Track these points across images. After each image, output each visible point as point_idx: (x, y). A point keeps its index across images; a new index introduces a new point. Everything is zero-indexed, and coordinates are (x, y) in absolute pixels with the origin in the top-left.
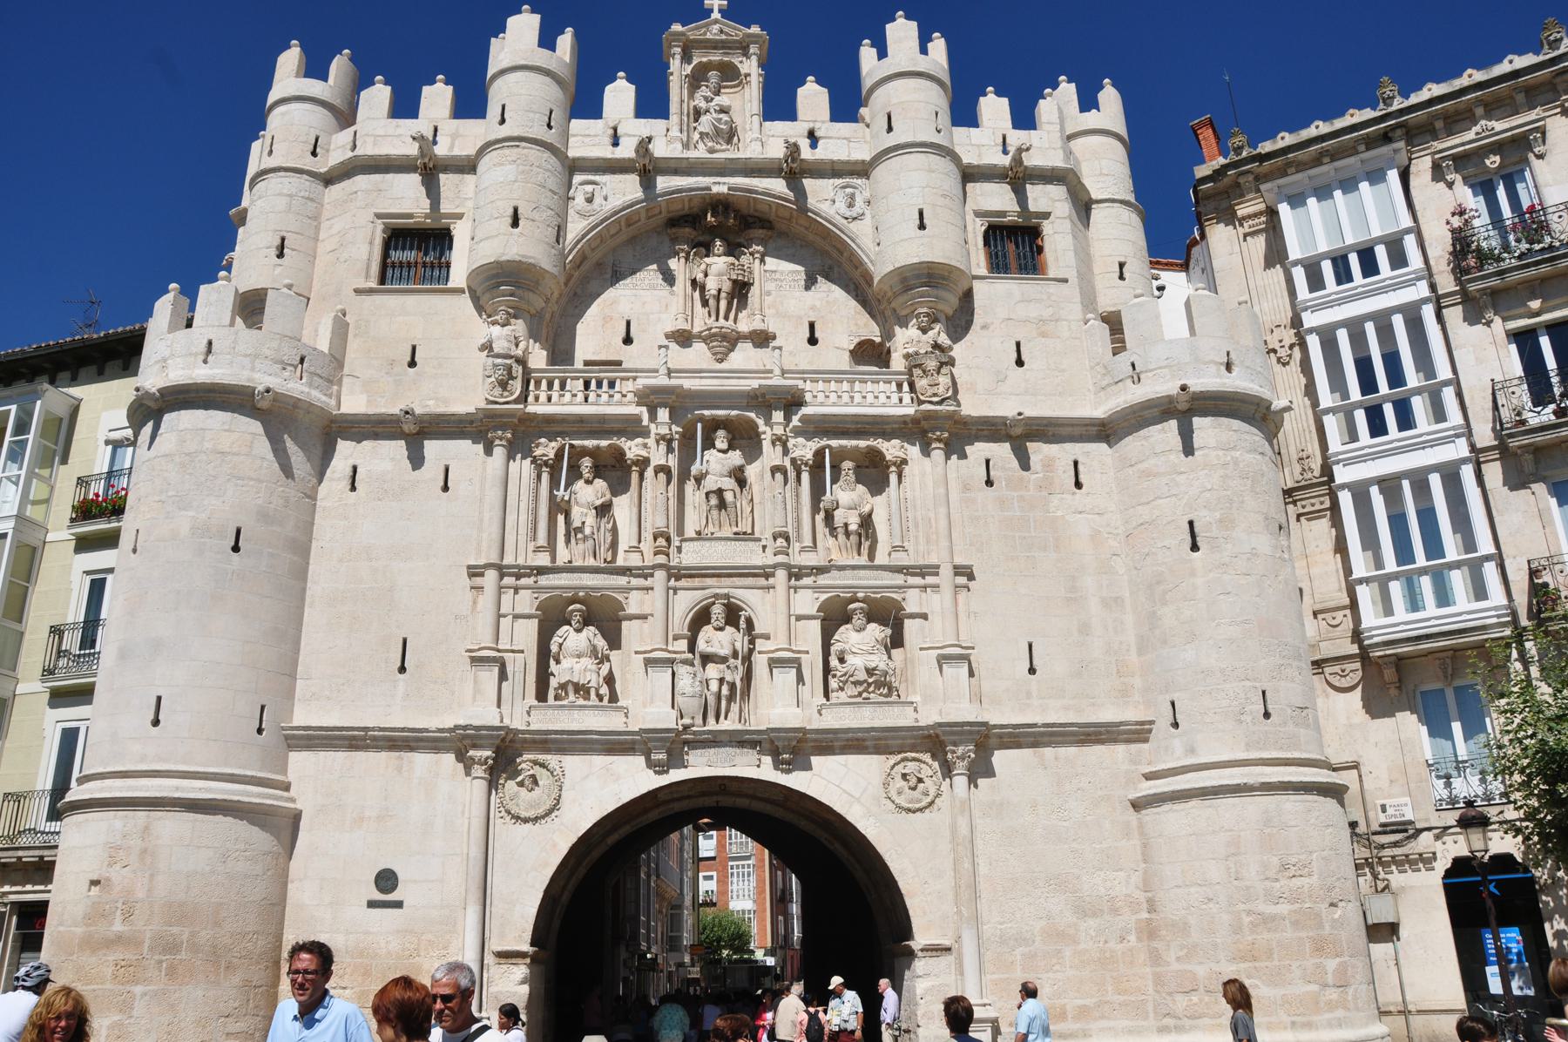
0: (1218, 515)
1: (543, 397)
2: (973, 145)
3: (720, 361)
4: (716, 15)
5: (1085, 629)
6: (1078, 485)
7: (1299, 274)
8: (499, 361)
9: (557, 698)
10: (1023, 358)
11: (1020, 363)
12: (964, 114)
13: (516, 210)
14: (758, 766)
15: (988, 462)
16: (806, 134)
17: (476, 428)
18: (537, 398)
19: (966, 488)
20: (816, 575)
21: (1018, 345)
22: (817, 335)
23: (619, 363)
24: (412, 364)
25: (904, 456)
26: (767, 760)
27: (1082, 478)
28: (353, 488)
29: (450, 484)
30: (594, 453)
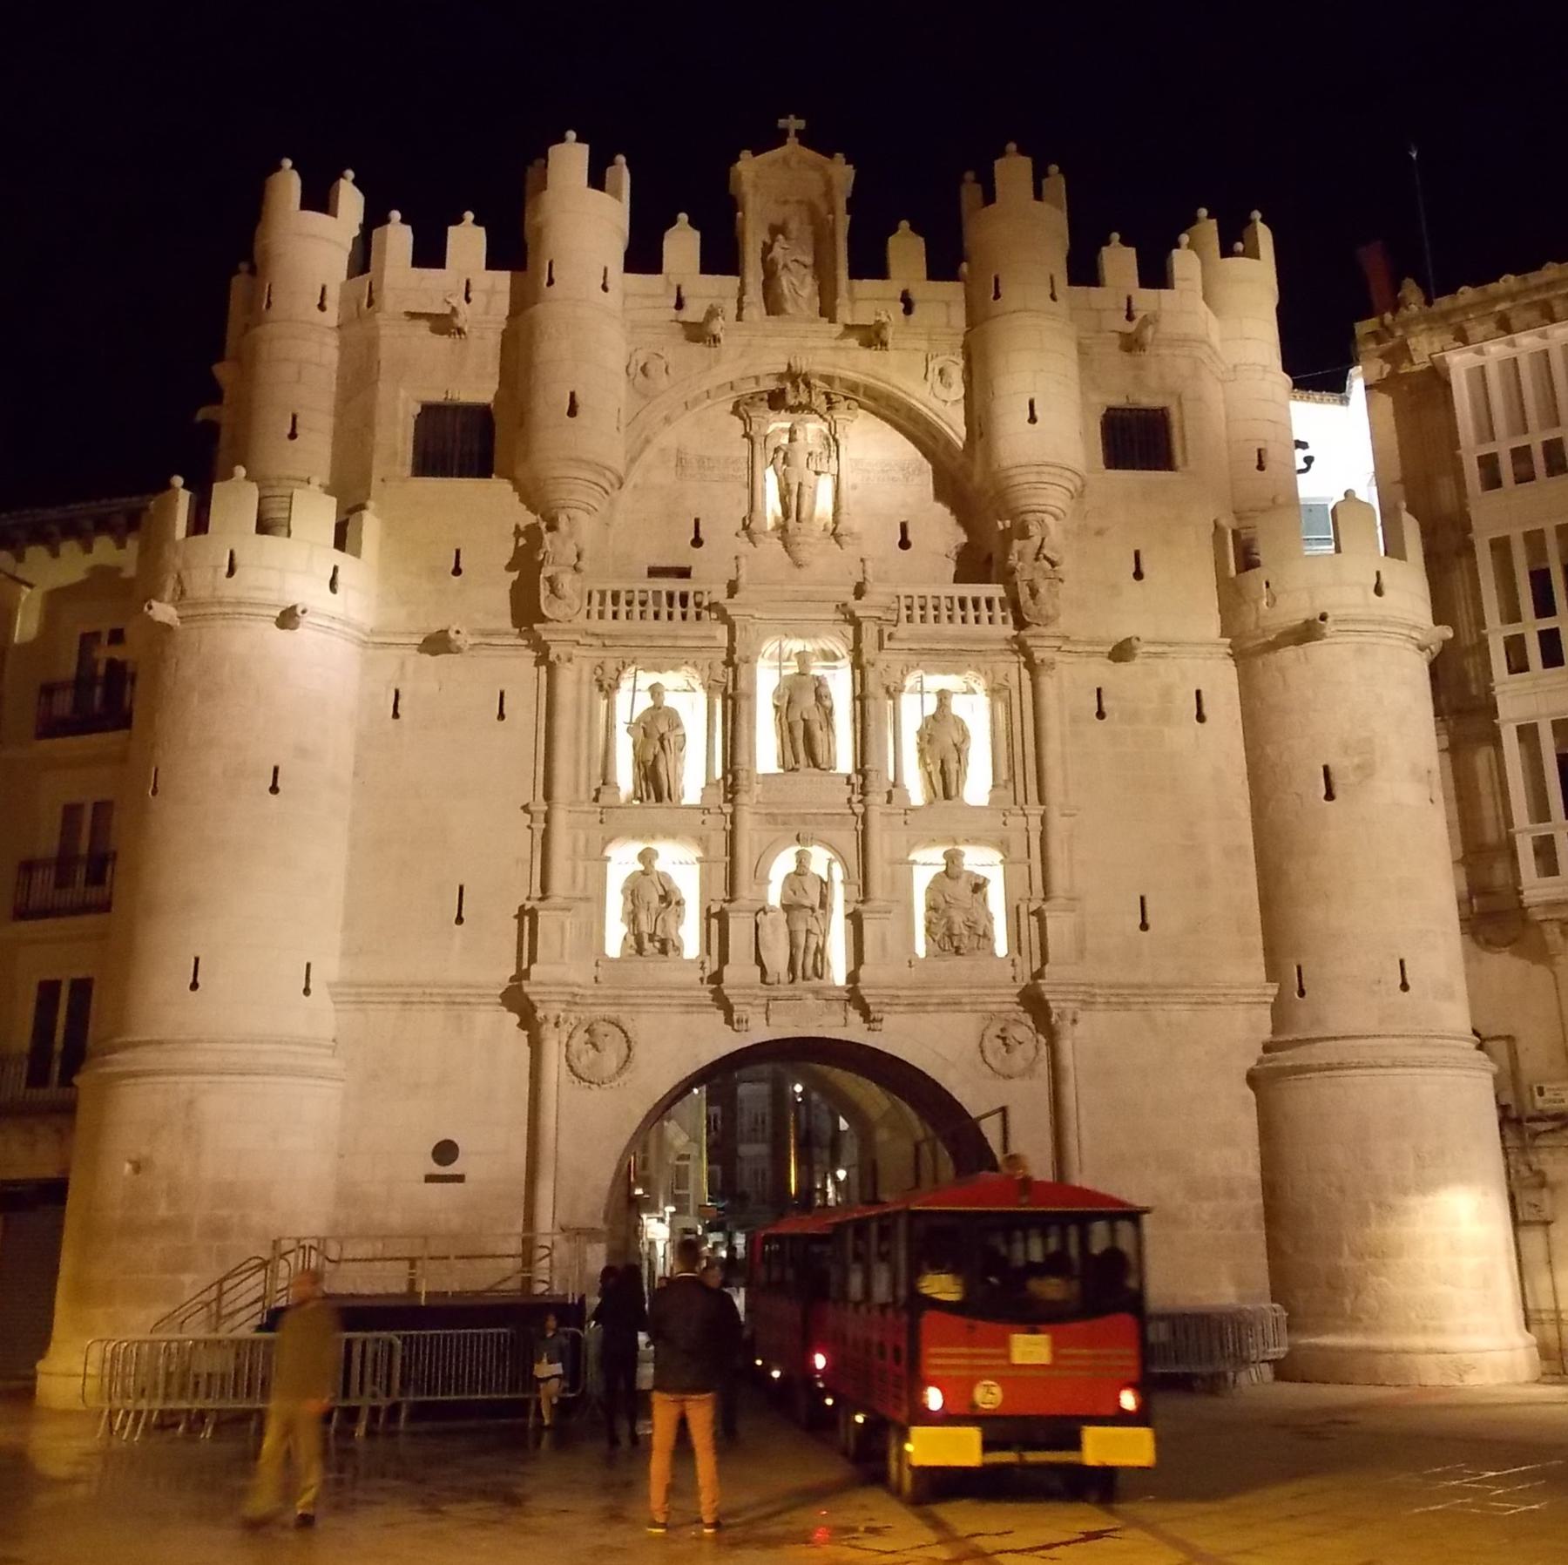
0: (1356, 760)
1: (609, 615)
2: (1091, 309)
4: (792, 141)
5: (1202, 882)
6: (1201, 718)
10: (1145, 568)
11: (1138, 575)
12: (1084, 271)
13: (572, 395)
14: (845, 1026)
15: (1099, 691)
16: (899, 296)
19: (1074, 720)
20: (906, 814)
22: (910, 537)
23: (684, 573)
24: (457, 571)
25: (1006, 684)
26: (855, 1016)
27: (1205, 710)
28: (396, 715)
29: (505, 711)
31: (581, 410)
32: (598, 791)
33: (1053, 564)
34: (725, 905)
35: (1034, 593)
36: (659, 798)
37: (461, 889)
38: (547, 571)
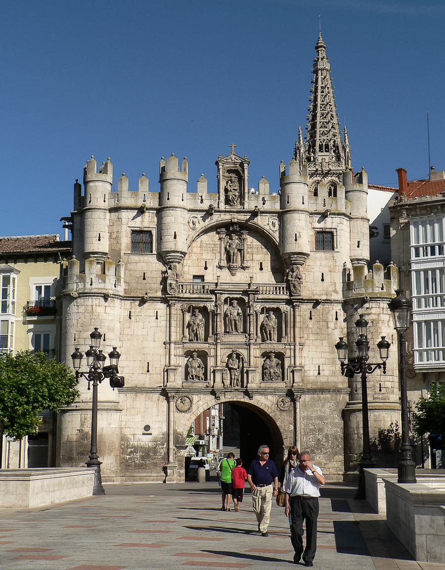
3: (233, 276)
7: (413, 251)
8: (172, 282)
9: (190, 378)
10: (324, 278)
11: (323, 280)
13: (175, 232)
17: (165, 300)
18: (182, 291)
21: (323, 274)
24: (144, 279)
30: (199, 308)
31: (177, 237)
32: (182, 339)
33: (299, 279)
34: (214, 368)
35: (295, 287)
36: (197, 340)
37: (148, 363)
38: (169, 282)
